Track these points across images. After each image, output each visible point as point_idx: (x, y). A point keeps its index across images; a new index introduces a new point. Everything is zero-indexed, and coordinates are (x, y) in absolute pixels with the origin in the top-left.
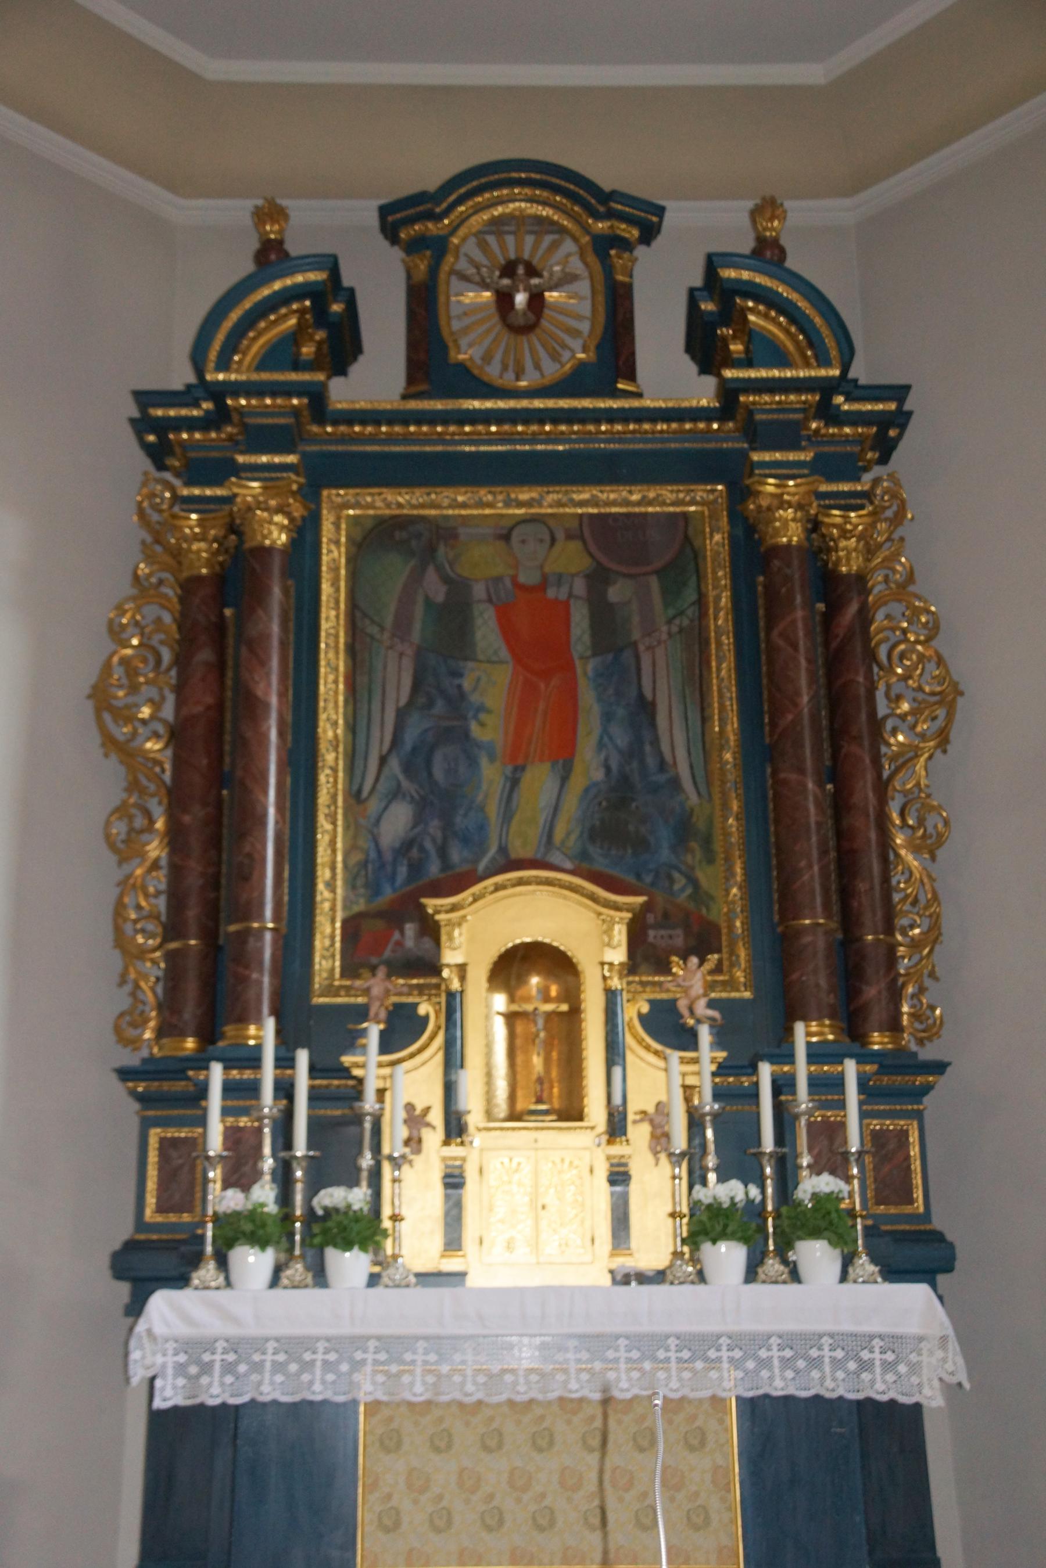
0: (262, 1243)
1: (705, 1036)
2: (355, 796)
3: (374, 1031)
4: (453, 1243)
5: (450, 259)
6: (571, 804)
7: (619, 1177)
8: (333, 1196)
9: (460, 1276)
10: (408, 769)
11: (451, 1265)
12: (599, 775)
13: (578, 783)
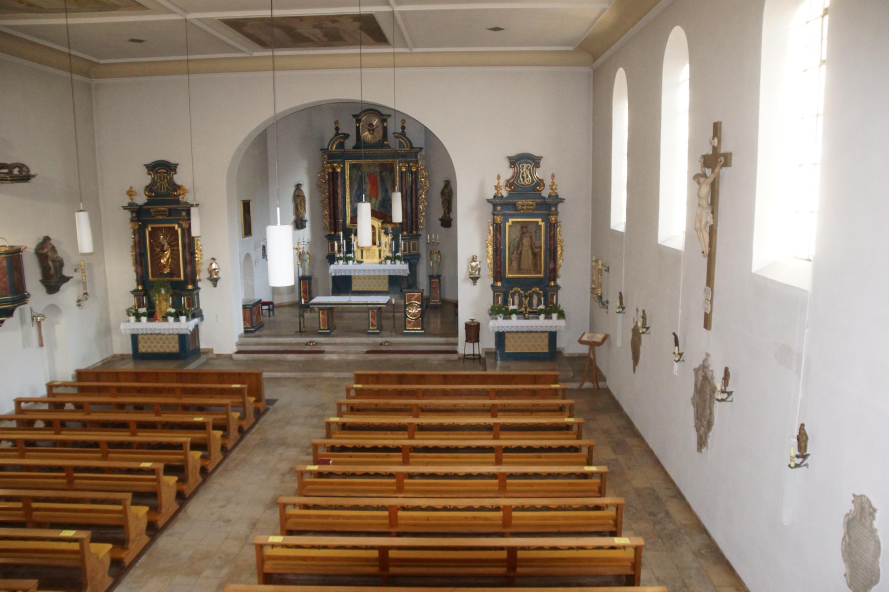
0: (341, 260)
1: (389, 235)
2: (351, 202)
3: (353, 235)
4: (362, 257)
5: (361, 124)
6: (378, 202)
7: (380, 251)
8: (349, 255)
9: (362, 262)
10: (357, 198)
11: (362, 260)
12: (381, 199)
13: (378, 200)
